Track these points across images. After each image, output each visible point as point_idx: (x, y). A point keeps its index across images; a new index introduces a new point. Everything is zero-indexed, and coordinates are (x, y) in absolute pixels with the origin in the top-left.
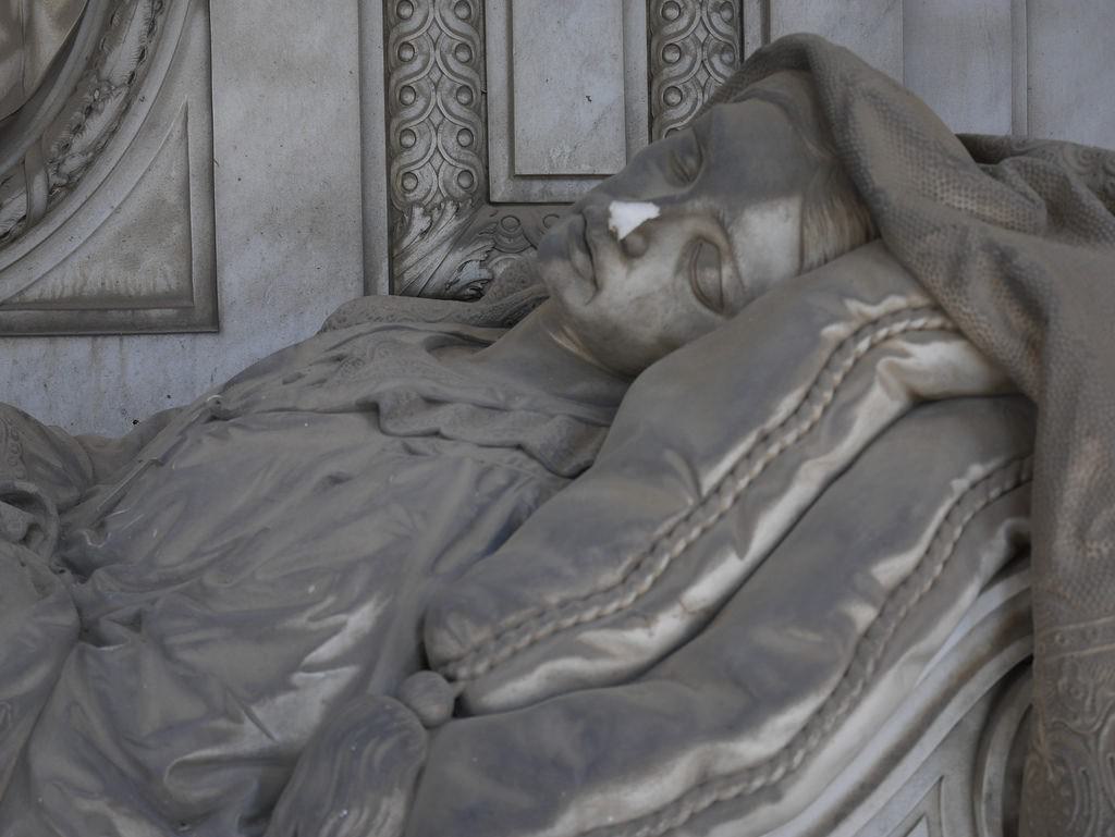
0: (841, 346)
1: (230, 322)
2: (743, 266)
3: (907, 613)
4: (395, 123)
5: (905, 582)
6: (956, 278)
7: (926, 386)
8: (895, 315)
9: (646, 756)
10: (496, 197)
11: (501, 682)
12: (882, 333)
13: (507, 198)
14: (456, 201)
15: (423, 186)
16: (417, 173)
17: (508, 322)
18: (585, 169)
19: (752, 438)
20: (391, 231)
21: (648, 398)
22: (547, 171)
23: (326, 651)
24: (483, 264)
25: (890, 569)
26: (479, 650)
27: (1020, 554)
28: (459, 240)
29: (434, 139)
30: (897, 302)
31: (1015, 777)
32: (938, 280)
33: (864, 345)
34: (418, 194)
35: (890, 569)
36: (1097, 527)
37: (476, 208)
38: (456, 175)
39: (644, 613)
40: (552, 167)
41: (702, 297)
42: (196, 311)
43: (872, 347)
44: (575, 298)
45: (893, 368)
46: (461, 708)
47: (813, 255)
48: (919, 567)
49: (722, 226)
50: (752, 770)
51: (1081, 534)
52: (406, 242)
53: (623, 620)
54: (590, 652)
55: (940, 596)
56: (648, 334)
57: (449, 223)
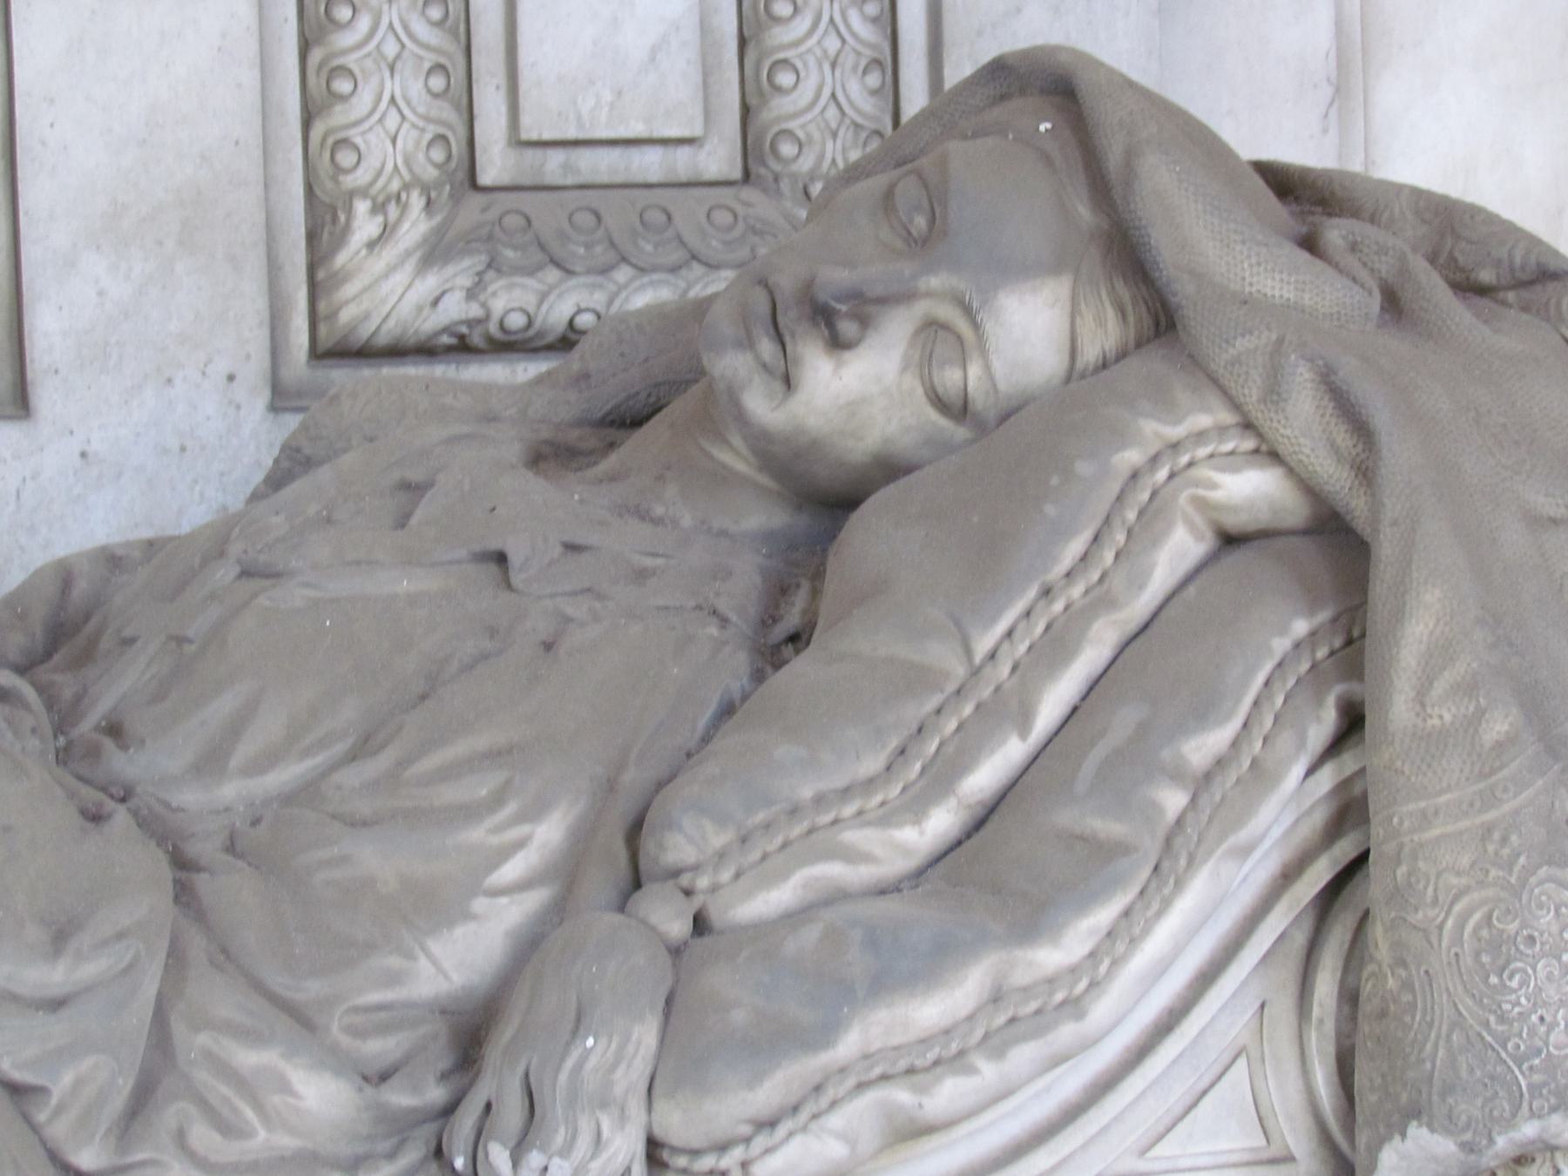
0: (1135, 476)
1: (46, 396)
2: (997, 365)
3: (1222, 791)
4: (316, 55)
5: (1220, 763)
6: (1274, 392)
7: (1234, 522)
8: (1200, 436)
10: (486, 177)
11: (749, 894)
12: (1184, 459)
13: (506, 179)
14: (426, 189)
15: (371, 163)
16: (358, 141)
17: (628, 420)
18: (637, 129)
19: (1032, 592)
20: (312, 237)
21: (871, 534)
22: (572, 133)
23: (511, 870)
24: (471, 294)
25: (1202, 747)
26: (722, 856)
27: (1352, 724)
28: (434, 253)
29: (388, 84)
30: (1203, 421)
31: (1350, 998)
32: (1251, 395)
33: (1162, 474)
34: (361, 177)
35: (1202, 747)
36: (1439, 687)
37: (456, 199)
38: (424, 143)
39: (915, 806)
40: (580, 125)
41: (939, 402)
43: (1172, 476)
44: (760, 404)
45: (1201, 504)
46: (700, 924)
47: (1090, 353)
48: (1235, 744)
49: (968, 311)
50: (1051, 981)
51: (1421, 698)
52: (341, 259)
53: (888, 817)
54: (851, 856)
55: (1261, 776)
56: (862, 445)
57: (415, 226)
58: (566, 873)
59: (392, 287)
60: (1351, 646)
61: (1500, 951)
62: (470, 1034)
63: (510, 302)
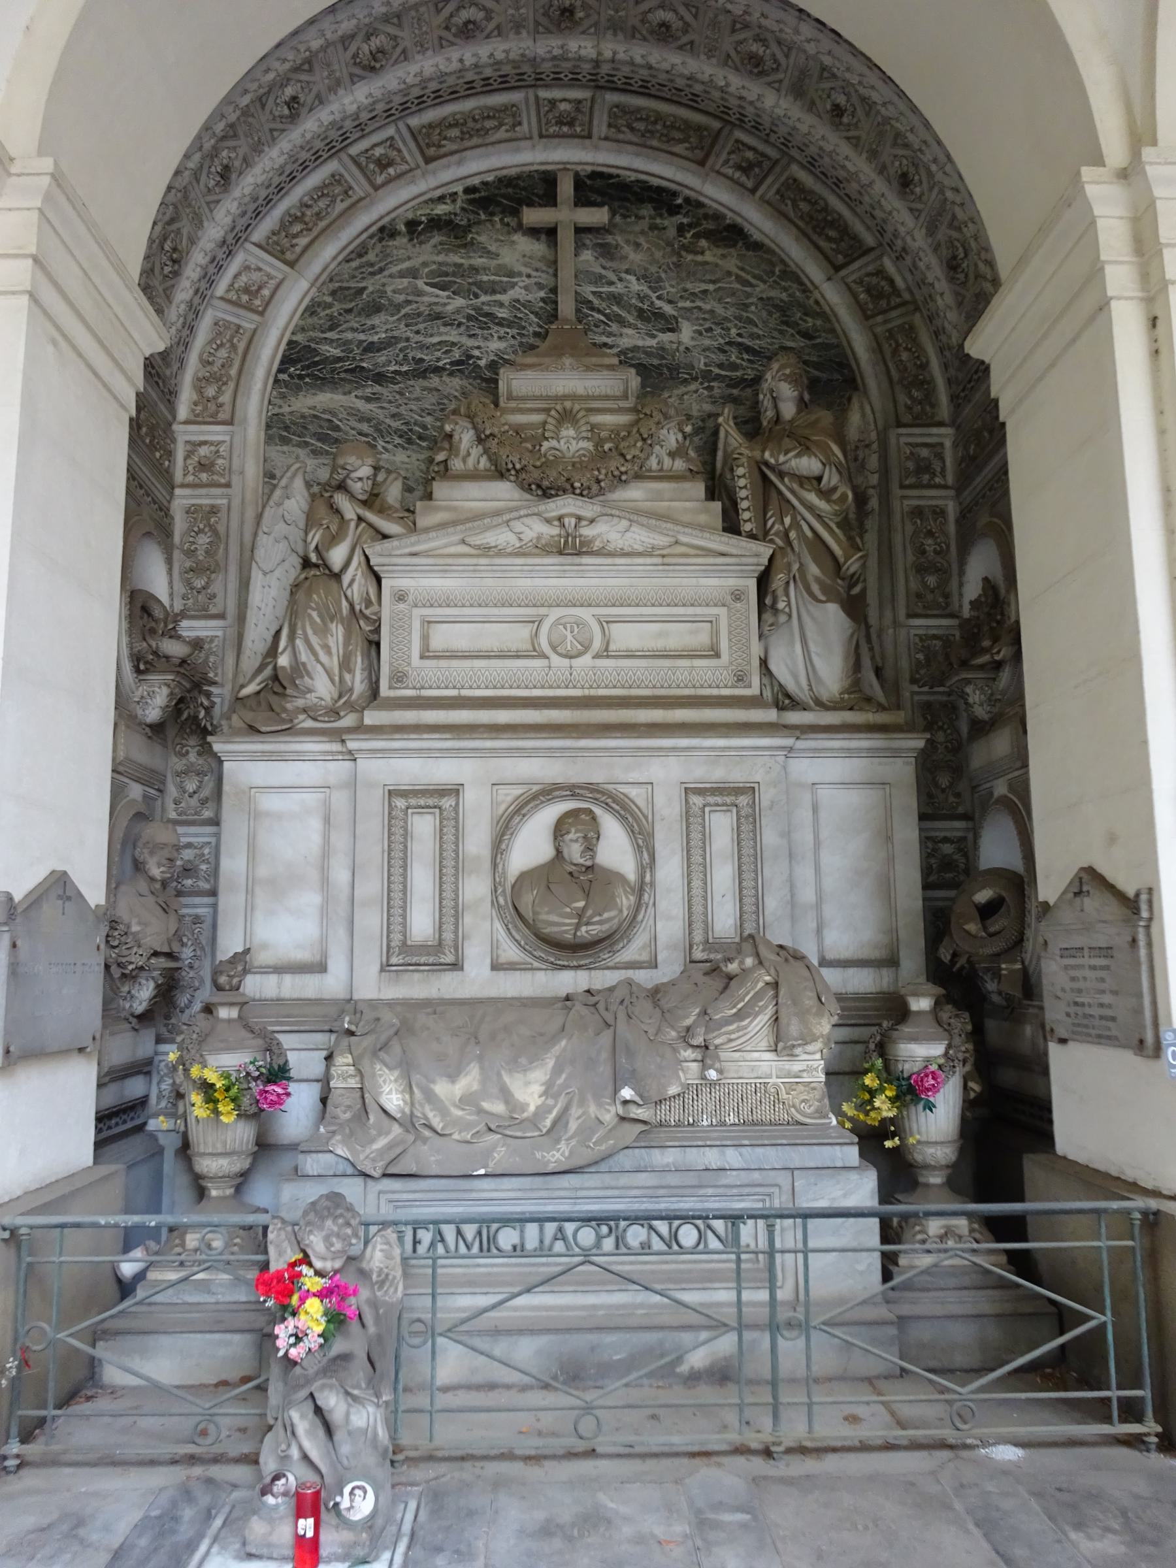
9: (731, 1023)
21: (733, 983)
42: (653, 964)
58: (699, 1015)
59: (699, 955)
60: (776, 996)
61: (788, 1025)
62: (688, 1029)
63: (712, 956)
